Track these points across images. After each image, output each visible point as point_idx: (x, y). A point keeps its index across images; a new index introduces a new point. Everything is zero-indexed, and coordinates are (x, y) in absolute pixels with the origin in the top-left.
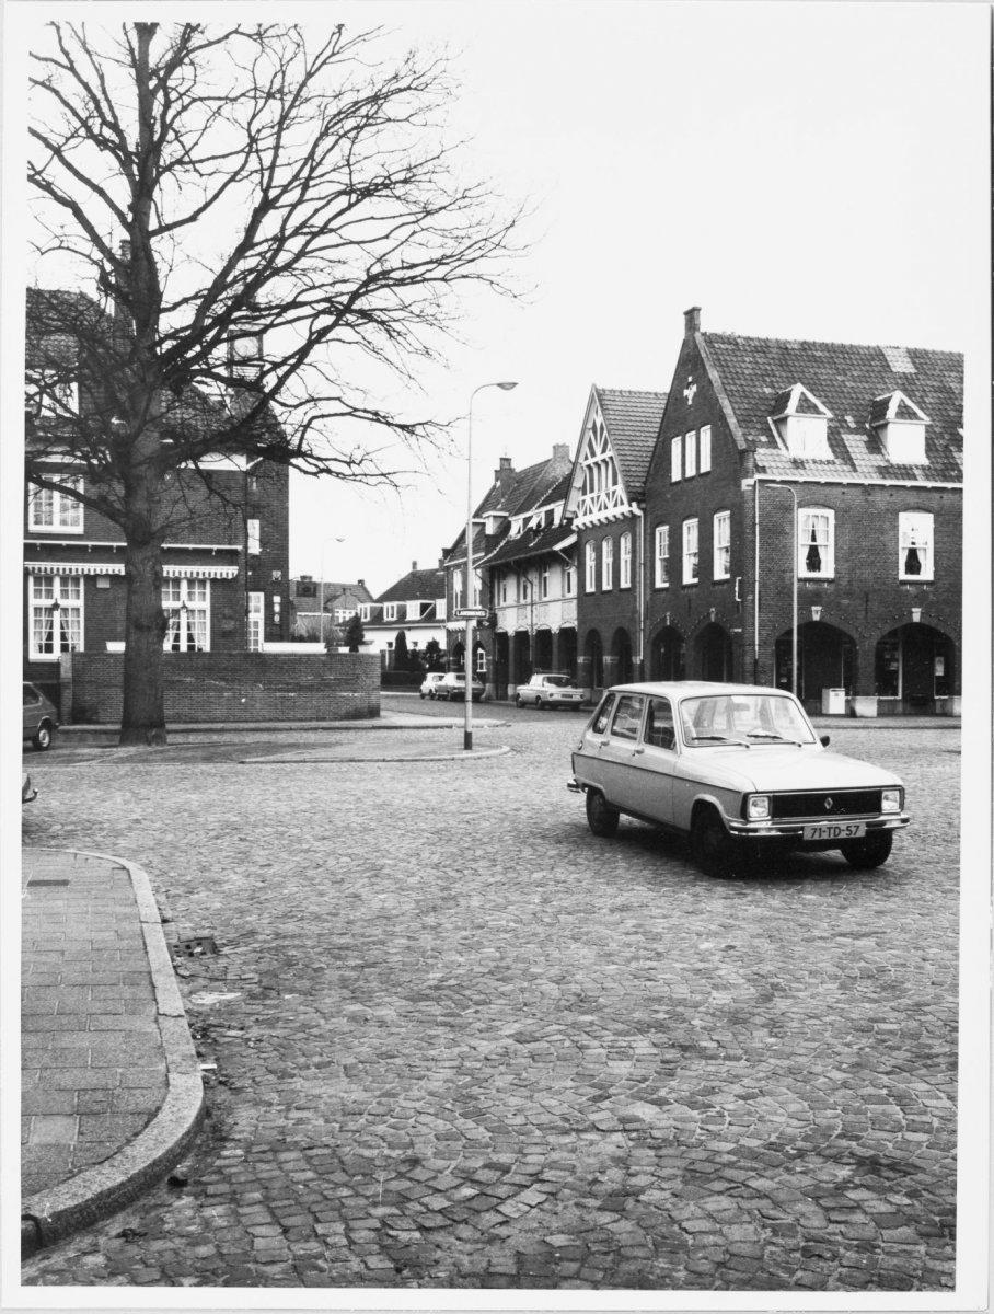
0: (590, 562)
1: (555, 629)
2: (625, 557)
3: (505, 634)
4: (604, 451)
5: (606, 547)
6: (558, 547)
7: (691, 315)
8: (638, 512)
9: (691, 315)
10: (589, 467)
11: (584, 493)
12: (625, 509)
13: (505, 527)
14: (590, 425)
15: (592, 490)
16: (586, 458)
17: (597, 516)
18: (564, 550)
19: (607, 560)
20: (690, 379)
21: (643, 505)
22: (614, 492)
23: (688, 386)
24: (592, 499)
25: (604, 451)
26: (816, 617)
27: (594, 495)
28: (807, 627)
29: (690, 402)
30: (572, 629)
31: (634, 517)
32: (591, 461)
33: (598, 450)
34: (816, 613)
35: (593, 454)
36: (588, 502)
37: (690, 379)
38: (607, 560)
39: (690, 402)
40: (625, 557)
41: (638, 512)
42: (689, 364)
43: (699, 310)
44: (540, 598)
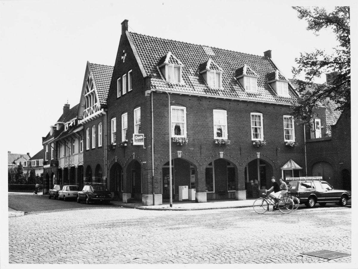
0: (88, 137)
2: (100, 133)
3: (61, 169)
4: (92, 89)
5: (93, 131)
6: (75, 131)
7: (125, 25)
8: (104, 113)
9: (125, 25)
10: (87, 97)
11: (85, 108)
12: (99, 112)
16: (86, 93)
17: (90, 117)
18: (77, 132)
19: (94, 135)
20: (124, 51)
21: (106, 110)
22: (96, 106)
23: (123, 55)
24: (88, 110)
25: (92, 89)
26: (180, 156)
27: (89, 108)
28: (177, 161)
29: (124, 62)
31: (103, 115)
33: (90, 89)
34: (180, 154)
35: (88, 91)
36: (87, 111)
37: (124, 51)
38: (94, 135)
39: (124, 62)
40: (100, 133)
41: (104, 113)
42: (124, 44)
44: (72, 154)
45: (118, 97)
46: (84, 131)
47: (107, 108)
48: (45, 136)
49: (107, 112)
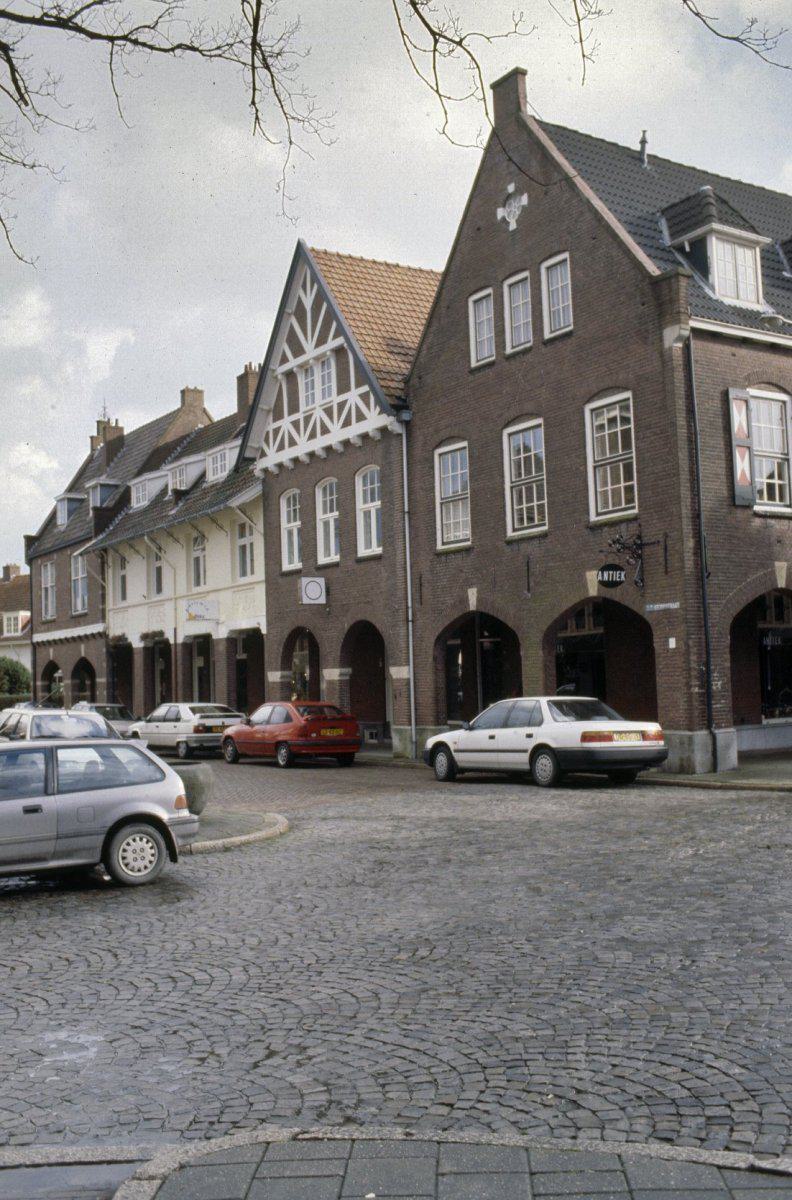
1: (221, 633)
7: (509, 90)
11: (278, 416)
13: (125, 498)
14: (292, 307)
15: (294, 409)
16: (284, 360)
17: (303, 448)
21: (406, 416)
23: (507, 199)
27: (299, 416)
29: (513, 226)
30: (256, 632)
32: (293, 363)
35: (298, 350)
37: (511, 188)
41: (397, 428)
43: (524, 73)
44: (189, 589)
45: (474, 364)
46: (268, 502)
47: (407, 408)
48: (34, 532)
49: (407, 424)
